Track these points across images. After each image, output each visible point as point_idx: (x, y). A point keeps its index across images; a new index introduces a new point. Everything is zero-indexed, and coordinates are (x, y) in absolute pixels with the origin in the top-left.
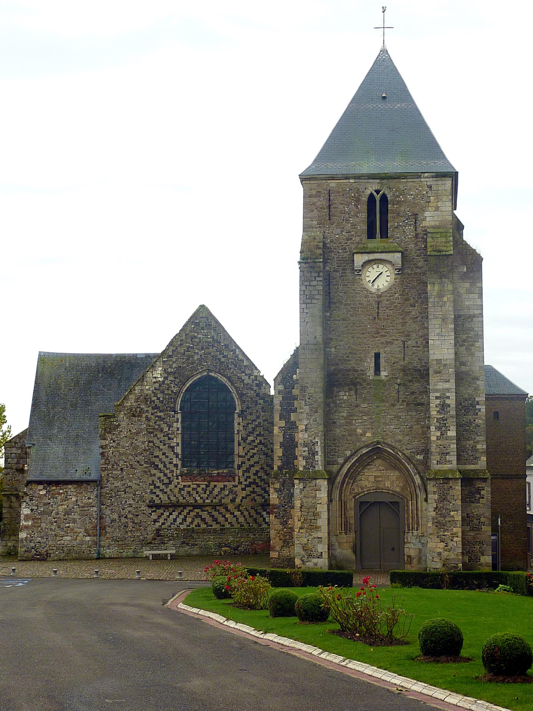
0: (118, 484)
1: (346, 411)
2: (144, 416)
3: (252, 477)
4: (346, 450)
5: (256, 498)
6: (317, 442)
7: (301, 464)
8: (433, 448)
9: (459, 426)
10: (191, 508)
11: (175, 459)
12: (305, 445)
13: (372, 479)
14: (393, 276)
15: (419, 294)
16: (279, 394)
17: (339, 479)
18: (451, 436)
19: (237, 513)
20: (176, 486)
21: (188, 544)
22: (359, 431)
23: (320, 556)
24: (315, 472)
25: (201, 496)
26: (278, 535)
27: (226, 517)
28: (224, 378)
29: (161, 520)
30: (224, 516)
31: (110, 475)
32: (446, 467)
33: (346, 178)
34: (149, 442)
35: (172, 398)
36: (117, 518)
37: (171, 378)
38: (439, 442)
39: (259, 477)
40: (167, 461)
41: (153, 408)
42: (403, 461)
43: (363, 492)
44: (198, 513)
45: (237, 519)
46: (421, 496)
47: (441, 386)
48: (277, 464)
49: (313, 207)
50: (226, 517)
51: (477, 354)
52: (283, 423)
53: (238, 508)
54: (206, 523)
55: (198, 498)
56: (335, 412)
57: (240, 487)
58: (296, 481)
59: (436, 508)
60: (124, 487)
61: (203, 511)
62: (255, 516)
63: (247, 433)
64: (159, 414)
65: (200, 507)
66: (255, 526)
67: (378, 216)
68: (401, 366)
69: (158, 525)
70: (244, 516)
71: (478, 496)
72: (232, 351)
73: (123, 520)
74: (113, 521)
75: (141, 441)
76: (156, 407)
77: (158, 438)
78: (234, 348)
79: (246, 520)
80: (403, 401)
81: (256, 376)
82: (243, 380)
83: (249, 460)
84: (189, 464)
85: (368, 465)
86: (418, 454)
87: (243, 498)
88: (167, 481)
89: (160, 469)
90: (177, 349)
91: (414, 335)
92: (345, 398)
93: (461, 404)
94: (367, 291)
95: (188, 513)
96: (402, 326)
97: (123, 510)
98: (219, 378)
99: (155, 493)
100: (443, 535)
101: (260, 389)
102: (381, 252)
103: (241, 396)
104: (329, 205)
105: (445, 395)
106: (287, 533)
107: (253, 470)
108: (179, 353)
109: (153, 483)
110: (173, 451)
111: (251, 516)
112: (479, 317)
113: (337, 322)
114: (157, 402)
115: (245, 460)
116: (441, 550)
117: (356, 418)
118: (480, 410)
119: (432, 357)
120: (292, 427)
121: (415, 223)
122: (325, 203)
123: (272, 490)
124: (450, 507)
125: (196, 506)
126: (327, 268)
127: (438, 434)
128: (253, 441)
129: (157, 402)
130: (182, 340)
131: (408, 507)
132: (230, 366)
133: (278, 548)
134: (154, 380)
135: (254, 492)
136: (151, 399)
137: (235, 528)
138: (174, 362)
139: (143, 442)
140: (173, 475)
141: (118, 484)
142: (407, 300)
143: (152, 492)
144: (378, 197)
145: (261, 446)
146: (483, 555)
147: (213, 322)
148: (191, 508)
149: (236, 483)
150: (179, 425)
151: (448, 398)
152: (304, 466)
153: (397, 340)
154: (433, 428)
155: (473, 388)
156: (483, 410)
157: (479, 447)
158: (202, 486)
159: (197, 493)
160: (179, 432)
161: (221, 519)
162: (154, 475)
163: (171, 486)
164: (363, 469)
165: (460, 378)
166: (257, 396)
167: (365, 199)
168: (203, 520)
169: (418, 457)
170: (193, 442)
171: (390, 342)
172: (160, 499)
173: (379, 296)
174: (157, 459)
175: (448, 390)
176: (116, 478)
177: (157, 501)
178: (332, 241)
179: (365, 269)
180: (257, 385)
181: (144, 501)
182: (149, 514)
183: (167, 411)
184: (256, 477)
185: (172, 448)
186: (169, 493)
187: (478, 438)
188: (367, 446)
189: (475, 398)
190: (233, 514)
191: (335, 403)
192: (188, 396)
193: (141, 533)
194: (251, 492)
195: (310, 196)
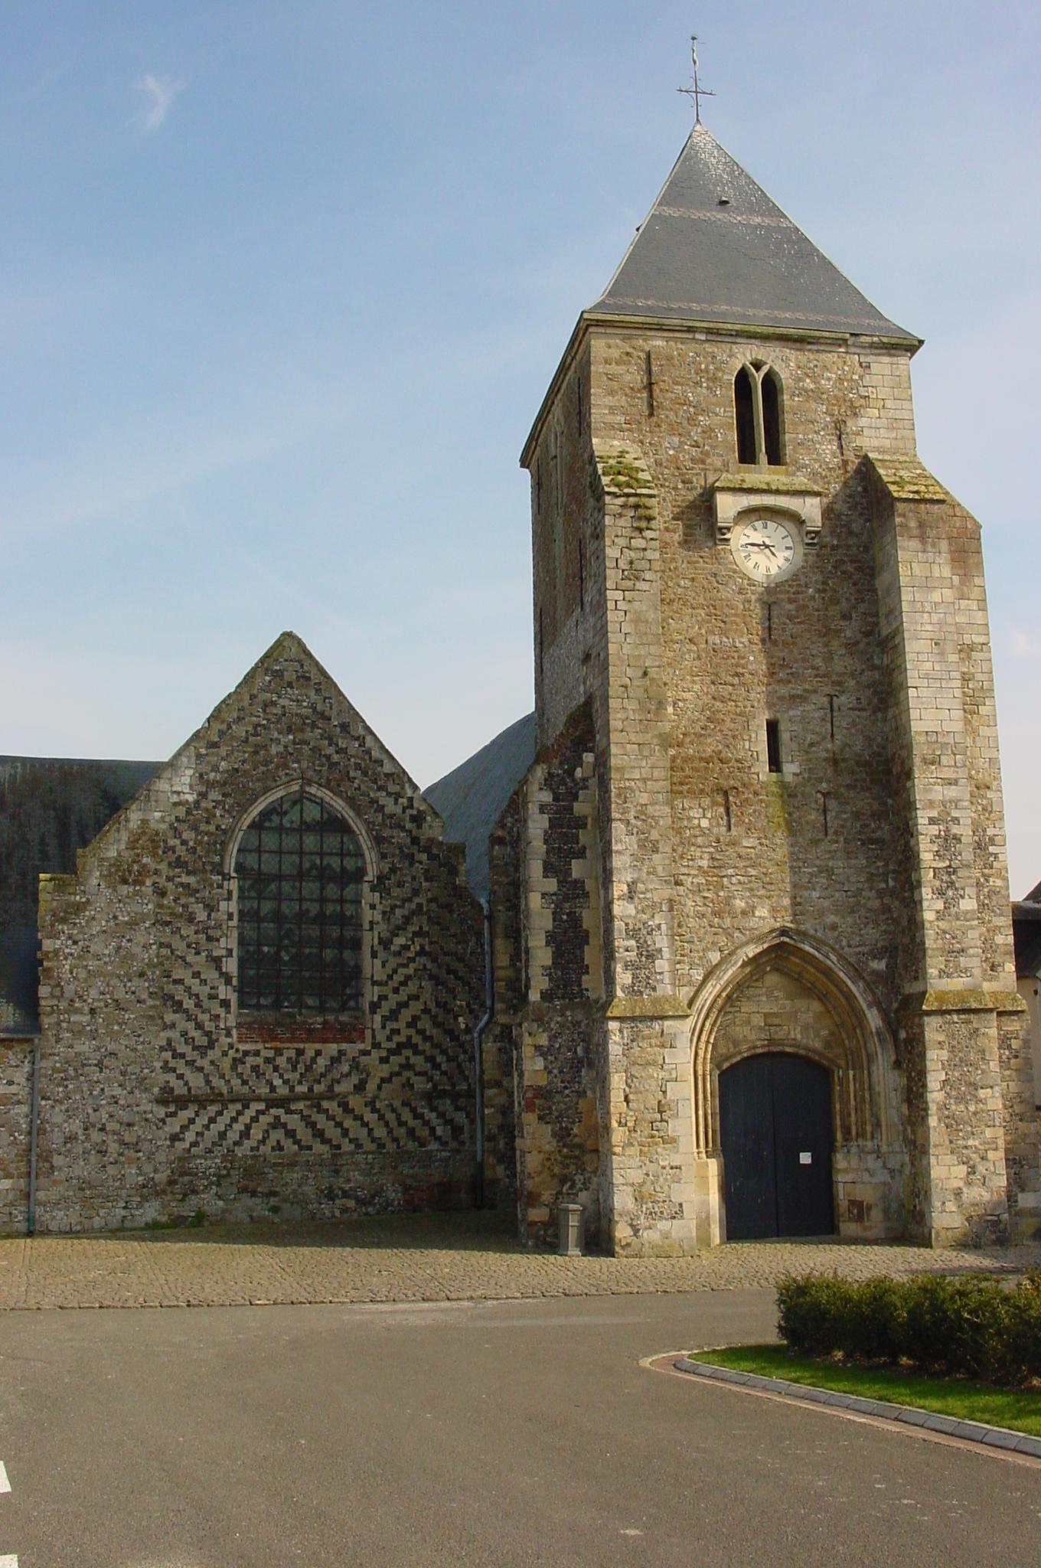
0: (84, 1046)
2: (148, 882)
5: (415, 1079)
6: (659, 927)
7: (623, 977)
10: (262, 1106)
11: (222, 988)
12: (632, 933)
13: (758, 1021)
14: (801, 550)
16: (542, 812)
19: (370, 1117)
22: (739, 904)
23: (677, 1214)
24: (656, 1001)
25: (286, 1077)
26: (548, 1164)
27: (346, 1125)
28: (340, 801)
29: (190, 1136)
30: (339, 1125)
31: (64, 1025)
32: (957, 983)
34: (161, 945)
35: (216, 843)
36: (80, 1132)
37: (215, 795)
38: (942, 924)
41: (170, 864)
44: (277, 1118)
45: (370, 1131)
47: (939, 793)
48: (538, 985)
50: (346, 1125)
51: (984, 731)
52: (551, 884)
53: (371, 1104)
54: (297, 1142)
55: (278, 1082)
57: (375, 1054)
61: (289, 1112)
63: (392, 927)
64: (185, 879)
65: (283, 1103)
66: (411, 1146)
68: (827, 751)
70: (387, 1124)
72: (357, 739)
73: (96, 1136)
74: (71, 1138)
75: (143, 944)
76: (179, 863)
78: (361, 732)
79: (390, 1132)
80: (836, 833)
81: (411, 799)
82: (383, 807)
83: (396, 991)
84: (254, 1001)
86: (874, 958)
87: (383, 1080)
88: (205, 1041)
89: (186, 1011)
90: (229, 727)
92: (705, 823)
94: (745, 576)
95: (255, 1119)
97: (95, 1111)
98: (327, 799)
100: (966, 1147)
101: (419, 827)
102: (778, 492)
103: (379, 840)
104: (650, 384)
105: (949, 814)
106: (571, 1157)
107: (406, 1015)
108: (233, 738)
109: (169, 1045)
110: (219, 968)
111: (401, 1124)
114: (181, 851)
115: (387, 990)
116: (961, 1184)
117: (730, 871)
121: (840, 438)
123: (527, 1051)
124: (977, 1078)
127: (939, 905)
128: (406, 947)
129: (181, 851)
132: (352, 774)
134: (175, 798)
135: (407, 1066)
136: (165, 841)
137: (366, 1153)
138: (223, 759)
139: (146, 947)
140: (217, 1027)
141: (84, 1046)
143: (166, 1068)
145: (423, 960)
146: (1023, 1190)
147: (314, 671)
148: (262, 1106)
150: (233, 907)
157: (999, 939)
159: (276, 1069)
160: (235, 922)
161: (332, 1132)
162: (173, 1026)
163: (214, 1054)
168: (291, 1134)
170: (266, 949)
171: (799, 697)
172: (186, 1084)
174: (181, 988)
175: (956, 803)
176: (78, 1033)
177: (180, 1089)
181: (146, 1090)
182: (163, 1121)
183: (204, 871)
184: (412, 1031)
185: (217, 961)
186: (208, 1068)
189: (984, 831)
190: (361, 1119)
192: (254, 842)
193: (139, 1168)
194: (401, 1066)
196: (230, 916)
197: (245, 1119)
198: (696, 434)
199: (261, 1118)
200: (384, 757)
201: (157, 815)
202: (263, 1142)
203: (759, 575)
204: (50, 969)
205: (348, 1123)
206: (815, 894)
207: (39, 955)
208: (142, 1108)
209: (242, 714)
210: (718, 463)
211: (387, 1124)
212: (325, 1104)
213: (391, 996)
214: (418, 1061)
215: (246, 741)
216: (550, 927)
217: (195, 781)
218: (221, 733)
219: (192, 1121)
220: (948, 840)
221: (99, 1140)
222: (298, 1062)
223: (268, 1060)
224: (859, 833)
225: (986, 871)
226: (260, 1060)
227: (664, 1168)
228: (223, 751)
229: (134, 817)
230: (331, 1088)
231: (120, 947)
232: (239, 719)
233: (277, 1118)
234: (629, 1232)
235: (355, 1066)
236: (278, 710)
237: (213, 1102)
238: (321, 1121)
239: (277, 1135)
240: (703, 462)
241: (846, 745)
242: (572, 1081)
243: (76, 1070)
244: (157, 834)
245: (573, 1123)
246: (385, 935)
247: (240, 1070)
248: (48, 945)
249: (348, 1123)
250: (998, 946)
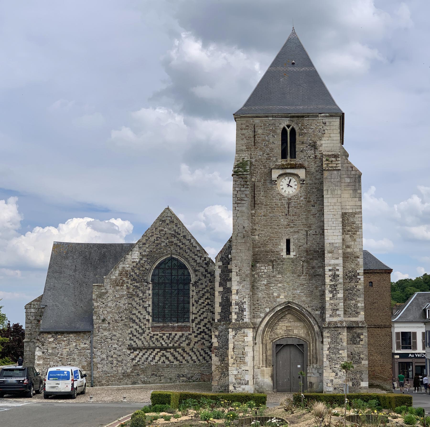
0: (106, 333)
1: (266, 280)
2: (125, 285)
3: (202, 328)
4: (266, 308)
5: (205, 342)
6: (245, 302)
7: (234, 317)
8: (327, 306)
9: (345, 290)
10: (159, 350)
11: (147, 316)
12: (237, 304)
13: (284, 328)
15: (317, 198)
16: (219, 268)
17: (261, 328)
18: (340, 297)
20: (148, 335)
21: (156, 375)
22: (275, 294)
23: (247, 384)
27: (184, 356)
29: (137, 359)
30: (182, 356)
33: (267, 117)
34: (129, 304)
36: (105, 358)
37: (145, 259)
38: (332, 302)
39: (207, 328)
40: (141, 317)
41: (131, 280)
42: (306, 315)
43: (279, 337)
44: (163, 353)
45: (191, 357)
46: (319, 340)
47: (333, 262)
48: (217, 317)
49: (243, 137)
50: (184, 356)
51: (358, 240)
52: (221, 289)
53: (192, 350)
54: (169, 361)
55: (163, 343)
56: (258, 281)
57: (193, 335)
58: (230, 330)
59: (329, 349)
60: (110, 336)
61: (167, 352)
62: (204, 355)
64: (136, 284)
65: (165, 349)
67: (289, 143)
69: (134, 362)
70: (196, 356)
71: (359, 339)
72: (189, 240)
73: (110, 359)
74: (103, 359)
76: (134, 279)
77: (135, 301)
78: (190, 238)
79: (198, 358)
80: (306, 273)
81: (205, 258)
83: (200, 316)
85: (282, 318)
87: (195, 342)
88: (141, 331)
89: (136, 323)
91: (314, 227)
92: (265, 271)
93: (346, 275)
94: (281, 195)
95: (156, 354)
96: (305, 220)
97: (110, 351)
98: (179, 259)
99: (133, 340)
100: (335, 368)
103: (195, 271)
104: (255, 135)
105: (335, 268)
107: (203, 323)
108: (150, 242)
112: (359, 214)
113: (259, 218)
114: (134, 276)
115: (197, 316)
116: (333, 378)
118: (360, 279)
119: (327, 242)
120: (227, 291)
122: (252, 134)
123: (213, 337)
124: (339, 347)
125: (162, 348)
126: (253, 180)
127: (331, 295)
128: (203, 303)
129: (134, 276)
130: (153, 233)
131: (310, 347)
133: (217, 378)
135: (203, 338)
136: (130, 273)
140: (145, 327)
142: (309, 202)
143: (130, 339)
144: (289, 130)
145: (207, 307)
146: (362, 381)
147: (175, 220)
148: (159, 350)
149: (191, 332)
150: (150, 292)
151: (338, 270)
152: (236, 319)
153: (302, 230)
154: (327, 292)
155: (355, 264)
156: (362, 279)
157: (359, 305)
158: (166, 335)
159: (163, 339)
160: (151, 297)
161: (180, 358)
164: (278, 321)
165: (346, 257)
166: (206, 271)
167: (279, 132)
168: (167, 358)
169: (317, 312)
170: (160, 304)
172: (136, 344)
173: (289, 199)
174: (135, 316)
175: (337, 265)
176: (105, 330)
177: (134, 345)
178: (256, 161)
179: (280, 180)
180: (206, 264)
181: (125, 345)
182: (129, 354)
183: (142, 282)
185: (146, 308)
186: (143, 339)
187: (358, 299)
188: (280, 305)
189: (356, 271)
190: (189, 354)
191: (257, 274)
195: (241, 129)
196: (149, 295)
197: (154, 354)
198: (268, 150)
199: (159, 354)
200: (196, 245)
201: (128, 266)
202: (159, 360)
203: (285, 194)
204: (96, 311)
205: (185, 355)
206: (298, 291)
207: (93, 307)
208: (124, 351)
209: (153, 234)
210: (274, 159)
211: (196, 356)
212: (177, 350)
213: (198, 317)
214: (206, 337)
215: (154, 242)
216: (221, 301)
217: (139, 255)
218: (147, 240)
219: (138, 354)
220: (335, 277)
221: (111, 360)
222: (170, 337)
223: (161, 337)
224: (314, 273)
225: (356, 284)
226: (158, 337)
227: (243, 370)
228: (147, 246)
229: (121, 266)
230: (179, 345)
231: (117, 305)
232: (152, 236)
233: (163, 353)
234: (233, 388)
235: (187, 338)
236: (164, 232)
237: (144, 349)
238: (176, 354)
239: (163, 358)
240: (270, 159)
241: (310, 246)
242: (225, 345)
243: (104, 340)
244: (127, 271)
245: (225, 357)
246: (197, 299)
247: (152, 340)
248: (95, 304)
249: (185, 355)
250: (359, 307)
